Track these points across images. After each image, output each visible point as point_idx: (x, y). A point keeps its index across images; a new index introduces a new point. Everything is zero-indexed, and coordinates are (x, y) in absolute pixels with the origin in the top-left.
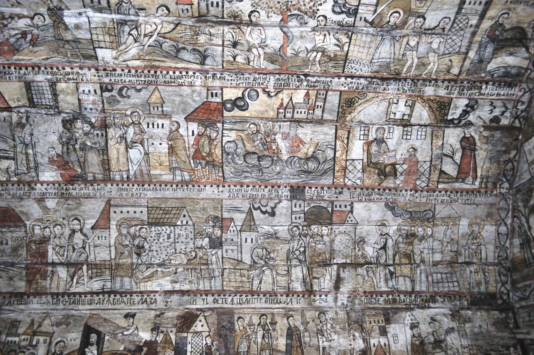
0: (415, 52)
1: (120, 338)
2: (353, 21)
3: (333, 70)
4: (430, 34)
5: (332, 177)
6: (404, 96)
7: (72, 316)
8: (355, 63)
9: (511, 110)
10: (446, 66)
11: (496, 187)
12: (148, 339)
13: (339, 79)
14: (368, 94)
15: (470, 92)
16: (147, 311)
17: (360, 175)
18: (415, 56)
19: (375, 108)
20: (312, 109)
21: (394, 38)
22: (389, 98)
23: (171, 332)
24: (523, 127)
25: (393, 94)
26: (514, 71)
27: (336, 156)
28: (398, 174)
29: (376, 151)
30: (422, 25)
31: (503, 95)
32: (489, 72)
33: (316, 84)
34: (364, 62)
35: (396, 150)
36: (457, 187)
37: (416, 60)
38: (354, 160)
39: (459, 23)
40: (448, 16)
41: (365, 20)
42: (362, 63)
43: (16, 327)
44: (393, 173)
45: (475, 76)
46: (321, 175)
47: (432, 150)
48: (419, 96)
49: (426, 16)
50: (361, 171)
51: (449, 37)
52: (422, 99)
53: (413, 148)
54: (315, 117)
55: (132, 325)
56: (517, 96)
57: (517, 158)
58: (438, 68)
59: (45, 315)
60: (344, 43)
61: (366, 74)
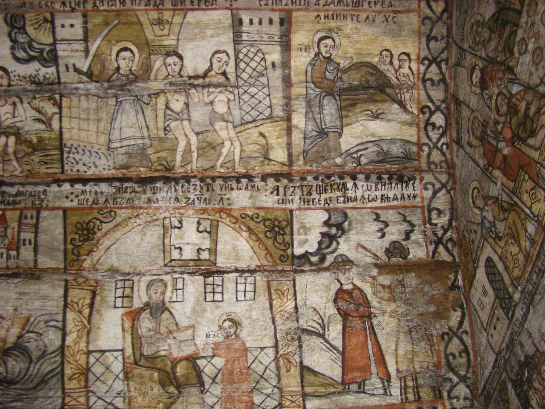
0: (186, 123)
2: (55, 73)
3: (43, 170)
4: (203, 87)
5: (60, 393)
6: (191, 212)
8: (82, 152)
10: (257, 147)
11: (441, 397)
13: (59, 186)
14: (118, 211)
15: (324, 196)
17: (119, 386)
18: (188, 131)
19: (138, 239)
20: (14, 247)
21: (138, 99)
22: (162, 216)
25: (167, 209)
26: (396, 150)
27: (67, 343)
28: (206, 379)
29: (150, 330)
30: (181, 70)
31: (395, 198)
32: (348, 154)
33: (18, 199)
34: (95, 149)
35: (193, 327)
36: (350, 405)
37: (194, 139)
38: (104, 352)
39: (247, 60)
40: (222, 49)
41: (76, 70)
42: (92, 150)
44: (194, 380)
45: (325, 163)
46: (34, 388)
47: (274, 322)
48: (221, 210)
49: (180, 52)
50: (121, 376)
51: (241, 91)
52: (229, 215)
53: (231, 320)
54: (22, 264)
56: (422, 198)
57: (466, 325)
58: (242, 151)
60: (50, 115)
61: (105, 172)
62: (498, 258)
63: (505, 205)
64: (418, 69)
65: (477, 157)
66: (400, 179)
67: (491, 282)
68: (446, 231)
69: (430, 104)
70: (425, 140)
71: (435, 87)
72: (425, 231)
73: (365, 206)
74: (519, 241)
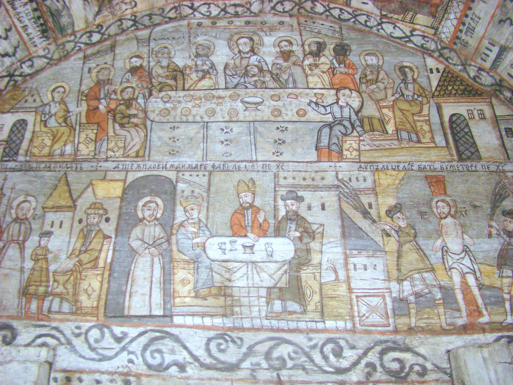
9: (15, 61)
24: (4, 93)
26: (64, 20)
31: (28, 35)
62: (32, 130)
63: (68, 121)
64: (127, 15)
65: (85, 82)
66: (44, 32)
67: (12, 131)
68: (21, 75)
69: (104, 29)
70: (78, 35)
71: (117, 28)
72: (14, 64)
73: (13, 18)
74: (56, 143)
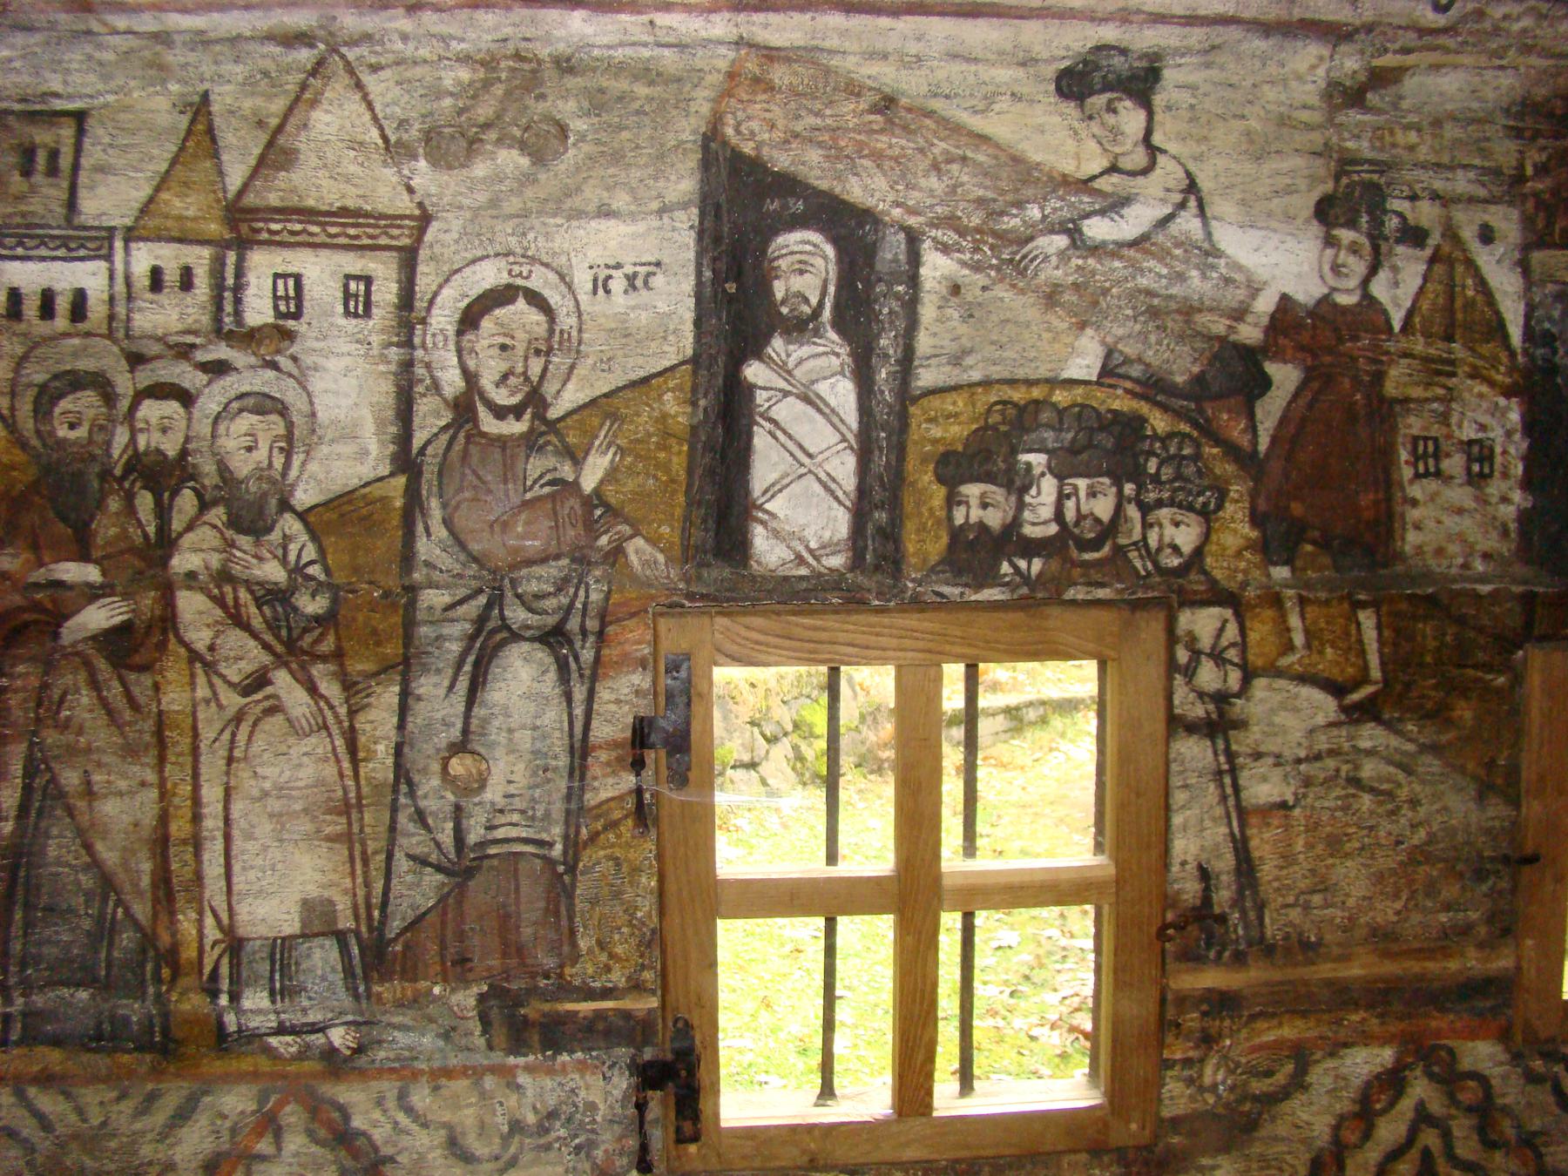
1: (1052, 273)
7: (566, 65)
12: (1307, 291)
16: (1259, 44)
23: (1487, 235)
43: (53, 170)
55: (1139, 158)
59: (305, 56)
